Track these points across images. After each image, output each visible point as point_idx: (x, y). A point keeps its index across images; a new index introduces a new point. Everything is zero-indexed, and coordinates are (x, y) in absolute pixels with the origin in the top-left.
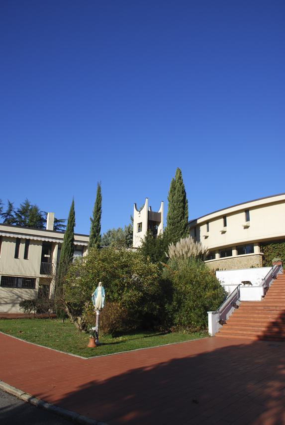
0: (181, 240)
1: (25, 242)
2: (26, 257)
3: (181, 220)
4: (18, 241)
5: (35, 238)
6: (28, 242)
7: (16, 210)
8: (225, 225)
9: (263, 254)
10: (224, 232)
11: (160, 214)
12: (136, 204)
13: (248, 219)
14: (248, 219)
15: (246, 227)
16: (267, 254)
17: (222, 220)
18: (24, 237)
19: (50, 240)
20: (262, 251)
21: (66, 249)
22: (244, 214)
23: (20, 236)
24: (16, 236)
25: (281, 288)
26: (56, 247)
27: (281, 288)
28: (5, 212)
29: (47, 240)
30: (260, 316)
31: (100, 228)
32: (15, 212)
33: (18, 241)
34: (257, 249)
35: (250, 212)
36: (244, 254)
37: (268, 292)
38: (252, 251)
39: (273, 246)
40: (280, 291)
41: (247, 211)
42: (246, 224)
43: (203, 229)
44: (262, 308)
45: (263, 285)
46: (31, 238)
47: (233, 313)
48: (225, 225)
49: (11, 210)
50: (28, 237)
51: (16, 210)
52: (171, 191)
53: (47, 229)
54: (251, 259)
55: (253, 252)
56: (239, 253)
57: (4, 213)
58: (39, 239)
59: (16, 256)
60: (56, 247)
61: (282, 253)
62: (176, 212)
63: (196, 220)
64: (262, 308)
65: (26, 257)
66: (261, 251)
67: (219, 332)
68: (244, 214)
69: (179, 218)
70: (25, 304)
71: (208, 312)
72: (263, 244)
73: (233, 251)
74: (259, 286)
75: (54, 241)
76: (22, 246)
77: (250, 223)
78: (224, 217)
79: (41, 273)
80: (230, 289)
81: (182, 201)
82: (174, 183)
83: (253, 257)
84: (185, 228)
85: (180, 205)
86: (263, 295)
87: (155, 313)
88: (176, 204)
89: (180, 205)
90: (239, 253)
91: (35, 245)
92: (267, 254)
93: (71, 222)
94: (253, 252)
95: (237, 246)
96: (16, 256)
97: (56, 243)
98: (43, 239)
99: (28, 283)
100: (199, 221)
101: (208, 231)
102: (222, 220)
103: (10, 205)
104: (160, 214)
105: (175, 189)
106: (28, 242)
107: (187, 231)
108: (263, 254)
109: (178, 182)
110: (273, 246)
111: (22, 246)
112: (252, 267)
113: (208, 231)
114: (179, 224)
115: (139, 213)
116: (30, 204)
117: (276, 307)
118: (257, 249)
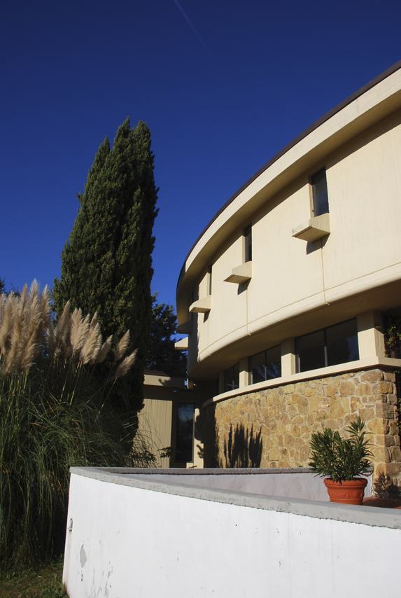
3: (104, 252)
13: (321, 206)
14: (321, 206)
34: (369, 343)
35: (330, 173)
36: (323, 366)
38: (351, 353)
54: (346, 391)
56: (304, 366)
62: (87, 227)
66: (388, 353)
69: (95, 247)
73: (283, 358)
77: (332, 222)
81: (112, 193)
83: (349, 380)
84: (114, 280)
90: (304, 366)
94: (356, 358)
107: (122, 290)
118: (369, 343)
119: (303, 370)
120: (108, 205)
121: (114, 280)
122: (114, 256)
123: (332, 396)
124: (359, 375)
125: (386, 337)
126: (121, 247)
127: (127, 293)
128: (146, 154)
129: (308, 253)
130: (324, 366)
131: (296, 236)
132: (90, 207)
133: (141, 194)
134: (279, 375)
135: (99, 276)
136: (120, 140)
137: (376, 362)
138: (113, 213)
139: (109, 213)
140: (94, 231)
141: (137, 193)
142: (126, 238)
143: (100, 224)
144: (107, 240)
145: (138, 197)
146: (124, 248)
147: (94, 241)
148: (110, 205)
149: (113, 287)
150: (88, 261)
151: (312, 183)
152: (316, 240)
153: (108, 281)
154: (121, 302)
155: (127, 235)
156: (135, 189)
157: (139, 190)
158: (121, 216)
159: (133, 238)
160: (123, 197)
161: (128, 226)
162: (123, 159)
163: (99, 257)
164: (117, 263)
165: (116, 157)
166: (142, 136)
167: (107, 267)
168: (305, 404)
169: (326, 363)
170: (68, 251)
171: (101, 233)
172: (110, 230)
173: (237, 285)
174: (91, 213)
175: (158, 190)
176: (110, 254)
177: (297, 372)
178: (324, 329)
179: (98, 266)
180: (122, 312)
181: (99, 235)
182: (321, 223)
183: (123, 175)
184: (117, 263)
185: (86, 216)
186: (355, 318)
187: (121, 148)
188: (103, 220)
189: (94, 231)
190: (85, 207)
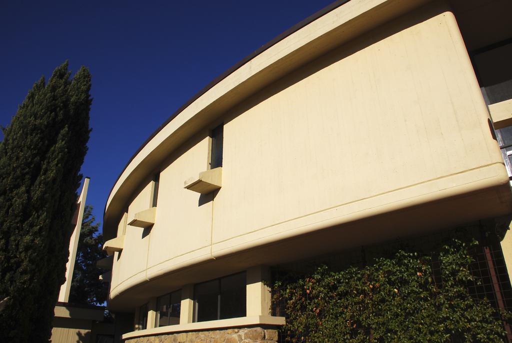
3: (17, 187)
9: (281, 321)
13: (216, 161)
14: (216, 161)
16: (299, 326)
20: (277, 308)
36: (216, 319)
39: (328, 280)
55: (243, 313)
56: (202, 314)
61: (373, 321)
77: (224, 177)
81: (35, 128)
84: (25, 213)
90: (202, 314)
94: (243, 313)
95: (196, 286)
107: (32, 225)
108: (281, 321)
119: (200, 320)
120: (29, 140)
121: (25, 213)
122: (28, 192)
124: (242, 332)
125: (273, 292)
126: (37, 182)
127: (36, 228)
128: (83, 96)
129: (199, 206)
130: (217, 319)
131: (189, 187)
132: (11, 141)
133: (67, 133)
134: (178, 323)
135: (7, 212)
136: (54, 80)
137: (258, 322)
138: (34, 149)
139: (29, 148)
140: (9, 165)
141: (63, 132)
142: (44, 174)
143: (18, 158)
144: (24, 175)
145: (63, 136)
146: (40, 184)
148: (32, 141)
149: (22, 222)
151: (212, 136)
152: (208, 193)
153: (16, 216)
154: (28, 238)
155: (46, 171)
156: (63, 127)
157: (66, 129)
158: (42, 152)
159: (51, 175)
160: (49, 133)
161: (49, 163)
162: (54, 98)
163: (11, 191)
164: (30, 198)
165: (45, 96)
166: (82, 80)
167: (17, 202)
169: (219, 318)
171: (17, 167)
172: (28, 165)
173: (142, 229)
174: (10, 147)
175: (91, 130)
176: (23, 189)
177: (194, 321)
178: (220, 279)
179: (9, 200)
180: (27, 249)
181: (14, 169)
182: (213, 178)
183: (51, 113)
184: (30, 198)
185: (5, 149)
187: (54, 89)
188: (21, 154)
189: (9, 165)
190: (7, 140)
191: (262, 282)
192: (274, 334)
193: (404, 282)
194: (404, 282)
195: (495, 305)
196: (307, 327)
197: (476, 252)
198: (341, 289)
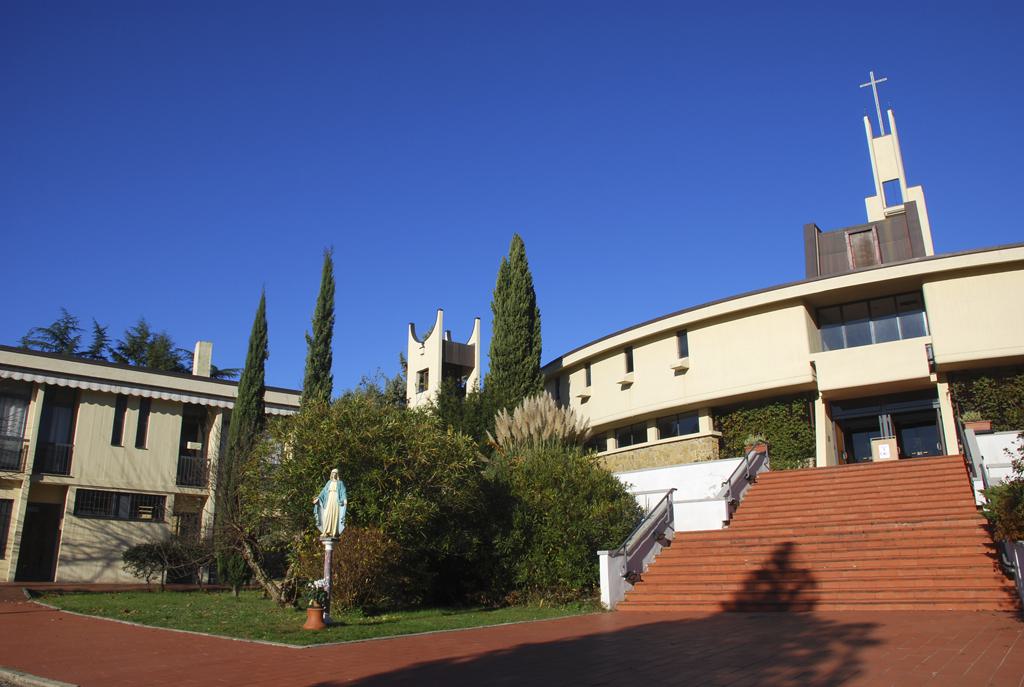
0: (526, 401)
1: (138, 405)
2: (140, 442)
3: (524, 357)
4: (121, 403)
5: (166, 396)
6: (146, 406)
7: (114, 345)
8: (630, 368)
9: (720, 434)
10: (626, 386)
11: (472, 347)
12: (413, 325)
15: (681, 371)
16: (731, 433)
17: (622, 357)
18: (136, 392)
19: (203, 401)
20: (717, 426)
21: (244, 414)
22: (674, 340)
23: (126, 391)
24: (115, 389)
25: (768, 503)
26: (218, 419)
27: (768, 503)
28: (86, 350)
29: (194, 400)
30: (723, 559)
31: (330, 360)
32: (111, 350)
33: (121, 403)
34: (705, 423)
35: (689, 334)
36: (675, 435)
37: (738, 511)
39: (745, 414)
40: (767, 509)
41: (681, 332)
42: (679, 362)
43: (577, 380)
44: (728, 542)
45: (726, 496)
46: (156, 395)
47: (657, 557)
48: (630, 368)
49: (102, 345)
50: (146, 393)
51: (114, 345)
52: (500, 289)
53: (195, 373)
54: (693, 448)
55: (698, 431)
56: (662, 435)
57: (83, 353)
58: (175, 397)
59: (116, 440)
60: (218, 419)
62: (511, 338)
63: (560, 359)
64: (728, 542)
65: (140, 442)
66: (714, 429)
67: (626, 600)
68: (674, 340)
69: (520, 353)
70: (138, 556)
71: (599, 553)
72: (720, 409)
73: (649, 430)
74: (717, 499)
75: (213, 403)
76: (131, 417)
77: (689, 362)
78: (627, 349)
79: (180, 482)
80: (648, 502)
81: (525, 312)
82: (506, 269)
83: (695, 442)
84: (533, 377)
85: (521, 320)
86: (725, 519)
87: (469, 555)
88: (511, 319)
89: (521, 320)
90: (662, 435)
91: (164, 412)
92: (731, 433)
93: (258, 346)
94: (698, 431)
95: (657, 419)
96: (116, 440)
97: (216, 410)
98: (185, 399)
99: (143, 504)
100: (566, 362)
101: (589, 383)
102: (622, 357)
103: (100, 333)
104: (473, 347)
105: (509, 283)
106: (146, 406)
107: (538, 383)
108: (720, 434)
109: (516, 268)
110: (745, 414)
111: (131, 417)
112: (696, 461)
113: (589, 383)
114: (518, 367)
115: (420, 345)
116: (150, 331)
117: (761, 538)
118: (705, 423)
123: (685, 450)
124: (700, 440)
134: (646, 441)
137: (710, 433)
147: (518, 349)
150: (516, 364)
151: (678, 336)
163: (523, 360)
168: (668, 456)
170: (497, 354)
181: (521, 345)
186: (697, 410)
191: (713, 418)
192: (717, 440)
193: (778, 415)
194: (778, 415)
195: (810, 421)
196: (734, 436)
197: (805, 403)
198: (750, 418)
